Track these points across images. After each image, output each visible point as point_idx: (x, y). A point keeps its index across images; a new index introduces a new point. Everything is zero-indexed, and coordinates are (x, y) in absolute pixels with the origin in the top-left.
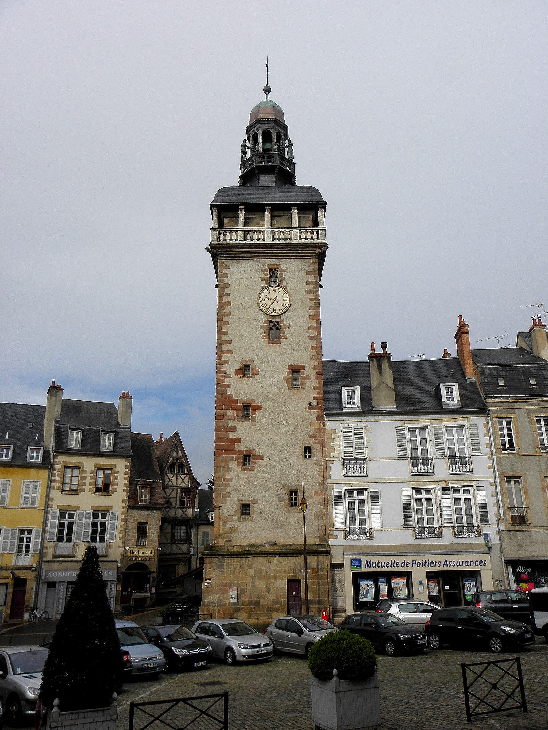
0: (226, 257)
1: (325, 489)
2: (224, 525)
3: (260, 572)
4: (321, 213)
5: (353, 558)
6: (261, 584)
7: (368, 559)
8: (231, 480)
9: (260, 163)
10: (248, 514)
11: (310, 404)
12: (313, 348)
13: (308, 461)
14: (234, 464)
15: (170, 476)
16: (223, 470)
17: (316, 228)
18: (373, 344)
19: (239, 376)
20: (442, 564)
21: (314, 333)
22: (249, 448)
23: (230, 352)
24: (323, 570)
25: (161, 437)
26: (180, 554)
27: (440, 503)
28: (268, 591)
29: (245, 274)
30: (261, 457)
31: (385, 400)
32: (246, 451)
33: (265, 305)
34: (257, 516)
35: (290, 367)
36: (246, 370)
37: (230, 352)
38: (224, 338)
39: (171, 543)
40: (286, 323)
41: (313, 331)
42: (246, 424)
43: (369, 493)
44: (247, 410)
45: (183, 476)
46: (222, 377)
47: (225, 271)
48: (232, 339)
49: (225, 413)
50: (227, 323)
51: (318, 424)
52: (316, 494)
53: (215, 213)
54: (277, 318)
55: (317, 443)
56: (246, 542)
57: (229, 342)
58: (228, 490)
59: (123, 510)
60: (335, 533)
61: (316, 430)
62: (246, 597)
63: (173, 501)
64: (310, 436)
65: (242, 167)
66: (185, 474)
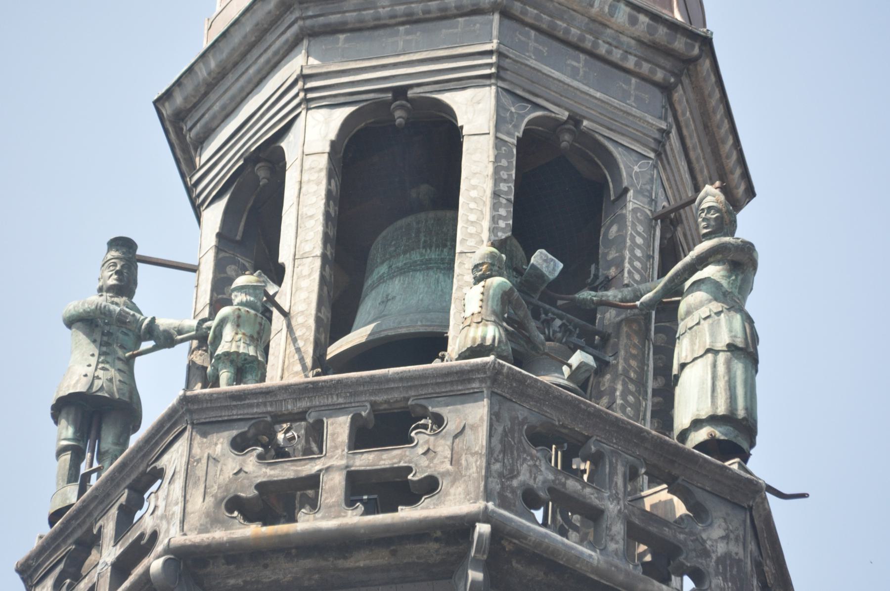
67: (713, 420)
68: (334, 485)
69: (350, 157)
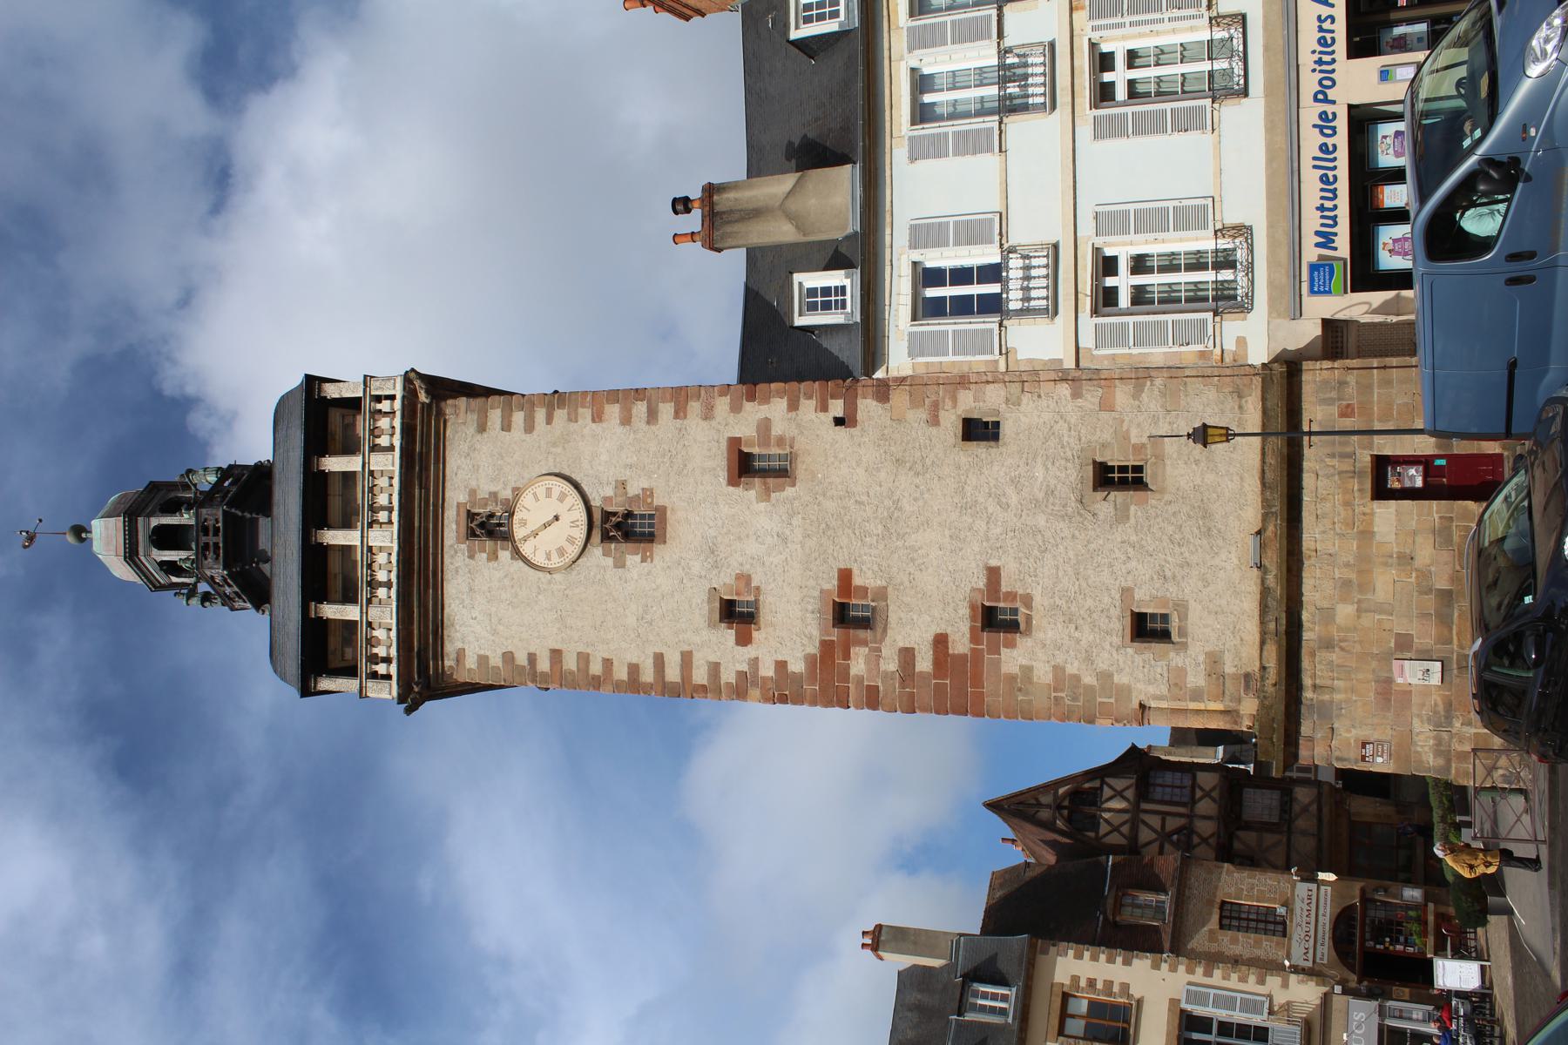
0: (435, 658)
1: (1095, 376)
2: (1197, 695)
3: (1347, 584)
4: (331, 391)
5: (1305, 287)
6: (1385, 583)
7: (1310, 240)
8: (1058, 670)
10: (1165, 617)
11: (839, 422)
12: (680, 413)
13: (1006, 430)
14: (1013, 657)
15: (1104, 828)
16: (1027, 693)
18: (676, 238)
19: (755, 634)
20: (1325, 11)
21: (640, 409)
22: (965, 611)
23: (687, 659)
24: (1342, 384)
25: (1013, 841)
26: (1320, 810)
27: (1138, 23)
28: (1406, 559)
29: (485, 611)
30: (993, 574)
31: (832, 197)
32: (973, 618)
34: (1173, 592)
35: (733, 482)
36: (737, 614)
37: (687, 659)
38: (648, 676)
39: (1290, 832)
40: (609, 492)
41: (634, 411)
42: (893, 618)
43: (1108, 239)
44: (850, 615)
45: (1107, 792)
46: (754, 684)
47: (471, 662)
48: (651, 650)
49: (860, 680)
50: (608, 663)
51: (899, 398)
52: (1106, 405)
53: (325, 684)
54: (597, 516)
55: (954, 400)
56: (1251, 629)
57: (659, 660)
58: (1089, 679)
59: (1182, 968)
60: (1230, 345)
61: (916, 403)
62: (1425, 635)
63: (1172, 823)
64: (934, 421)
65: (236, 605)
66: (1101, 788)
68: (215, 539)
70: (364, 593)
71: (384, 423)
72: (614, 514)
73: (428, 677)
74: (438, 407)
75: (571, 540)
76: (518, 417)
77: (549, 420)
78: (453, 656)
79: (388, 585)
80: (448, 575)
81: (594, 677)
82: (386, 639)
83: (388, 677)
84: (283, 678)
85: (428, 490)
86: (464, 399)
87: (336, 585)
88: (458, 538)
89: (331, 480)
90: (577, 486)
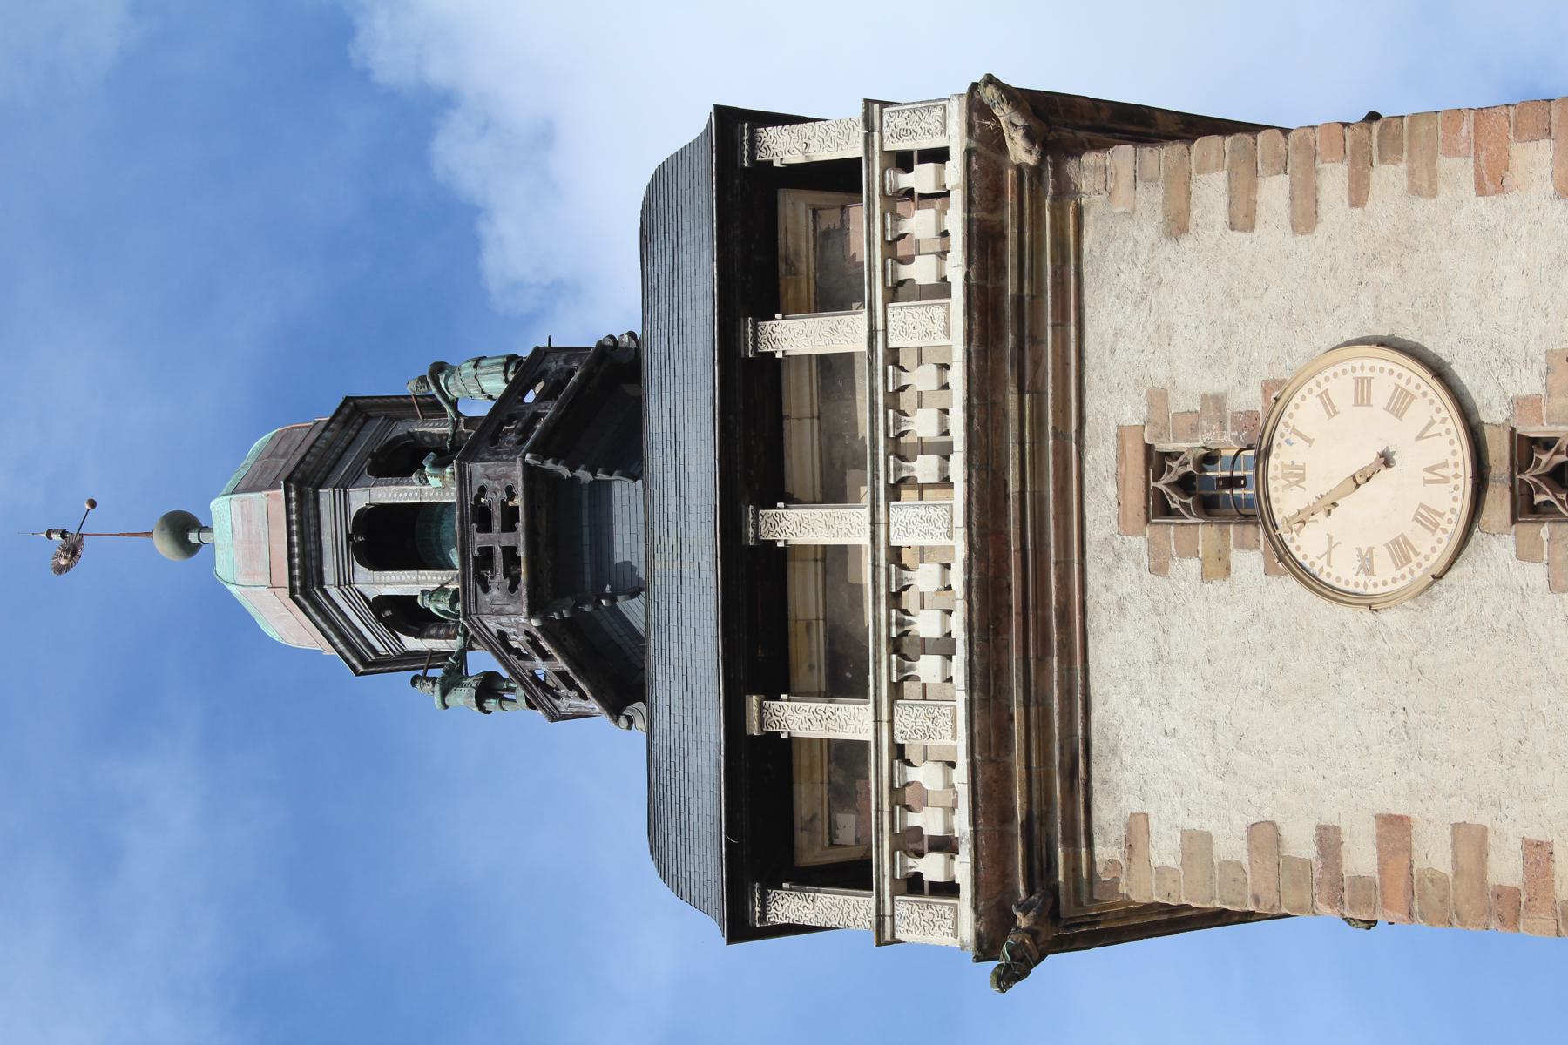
0: (1071, 840)
4: (783, 148)
9: (513, 588)
17: (875, 176)
29: (1197, 705)
33: (1401, 550)
40: (1530, 383)
47: (1164, 851)
53: (788, 906)
54: (1499, 453)
65: (563, 706)
67: (505, 372)
68: (507, 539)
69: (378, 560)
70: (882, 671)
71: (920, 223)
72: (1547, 444)
73: (1054, 891)
74: (1058, 173)
75: (1426, 518)
76: (1274, 192)
77: (1358, 194)
78: (1118, 833)
79: (945, 647)
80: (1098, 620)
81: (1501, 893)
82: (941, 794)
83: (948, 889)
84: (684, 892)
85: (1039, 394)
86: (1127, 149)
87: (810, 650)
88: (1122, 522)
89: (790, 379)
90: (1440, 372)
